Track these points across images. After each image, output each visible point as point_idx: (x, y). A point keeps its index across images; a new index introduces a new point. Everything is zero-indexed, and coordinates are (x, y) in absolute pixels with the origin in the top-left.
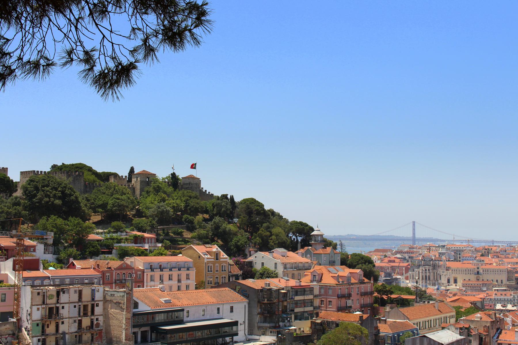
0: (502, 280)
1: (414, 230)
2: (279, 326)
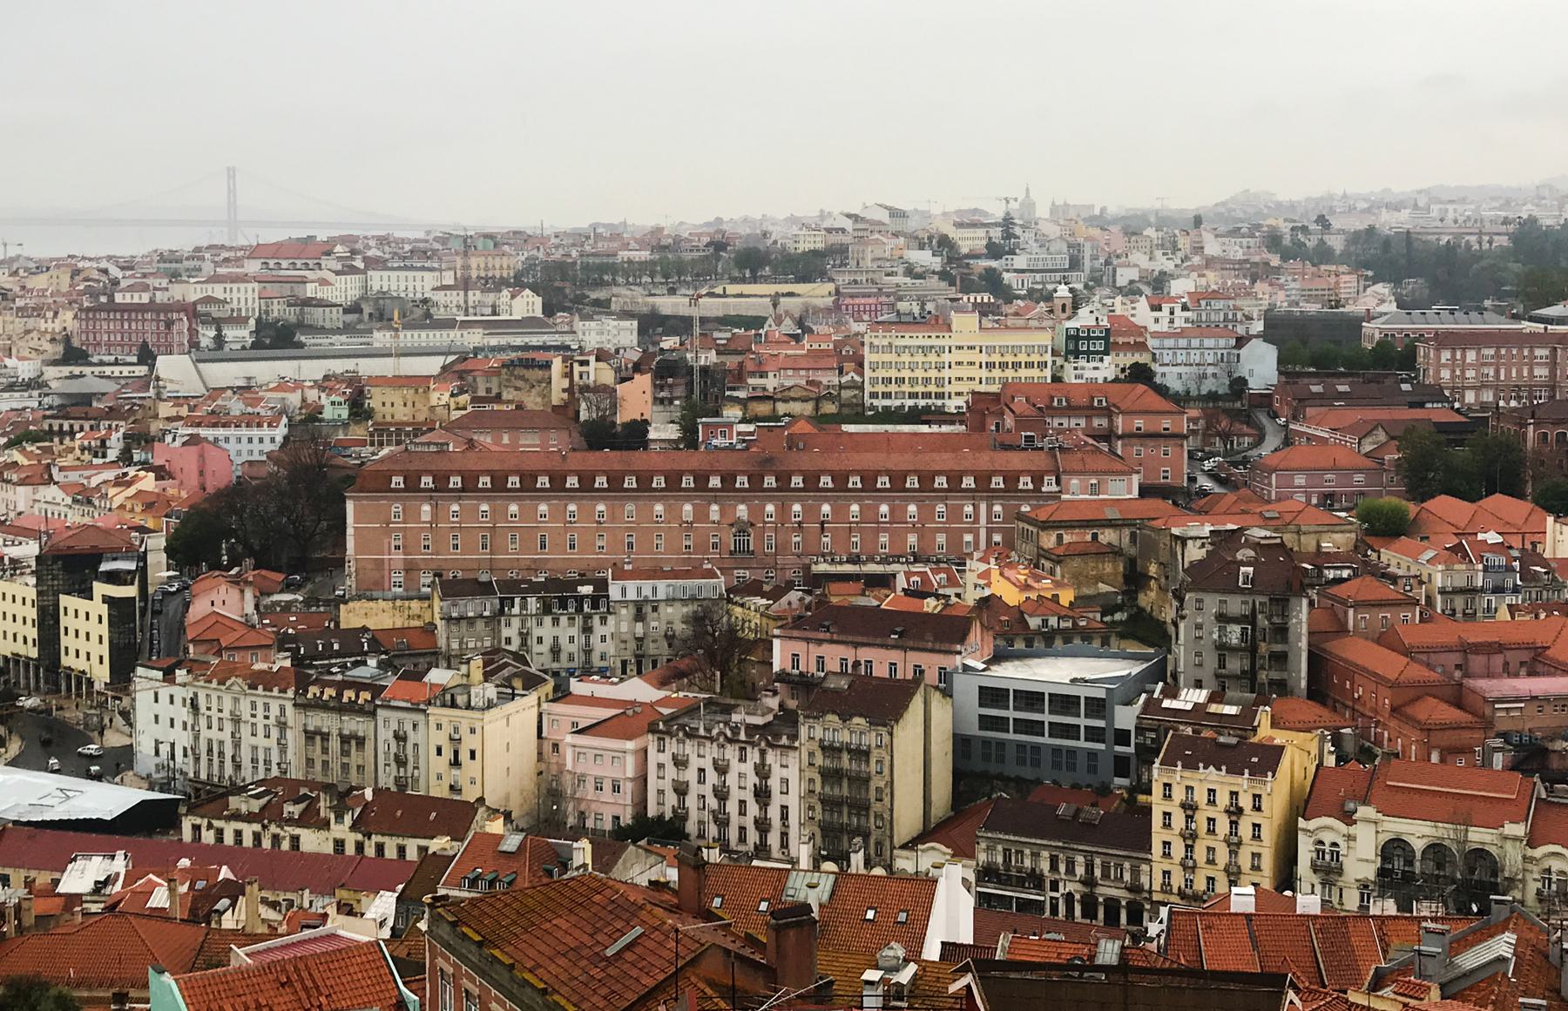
1: (232, 192)
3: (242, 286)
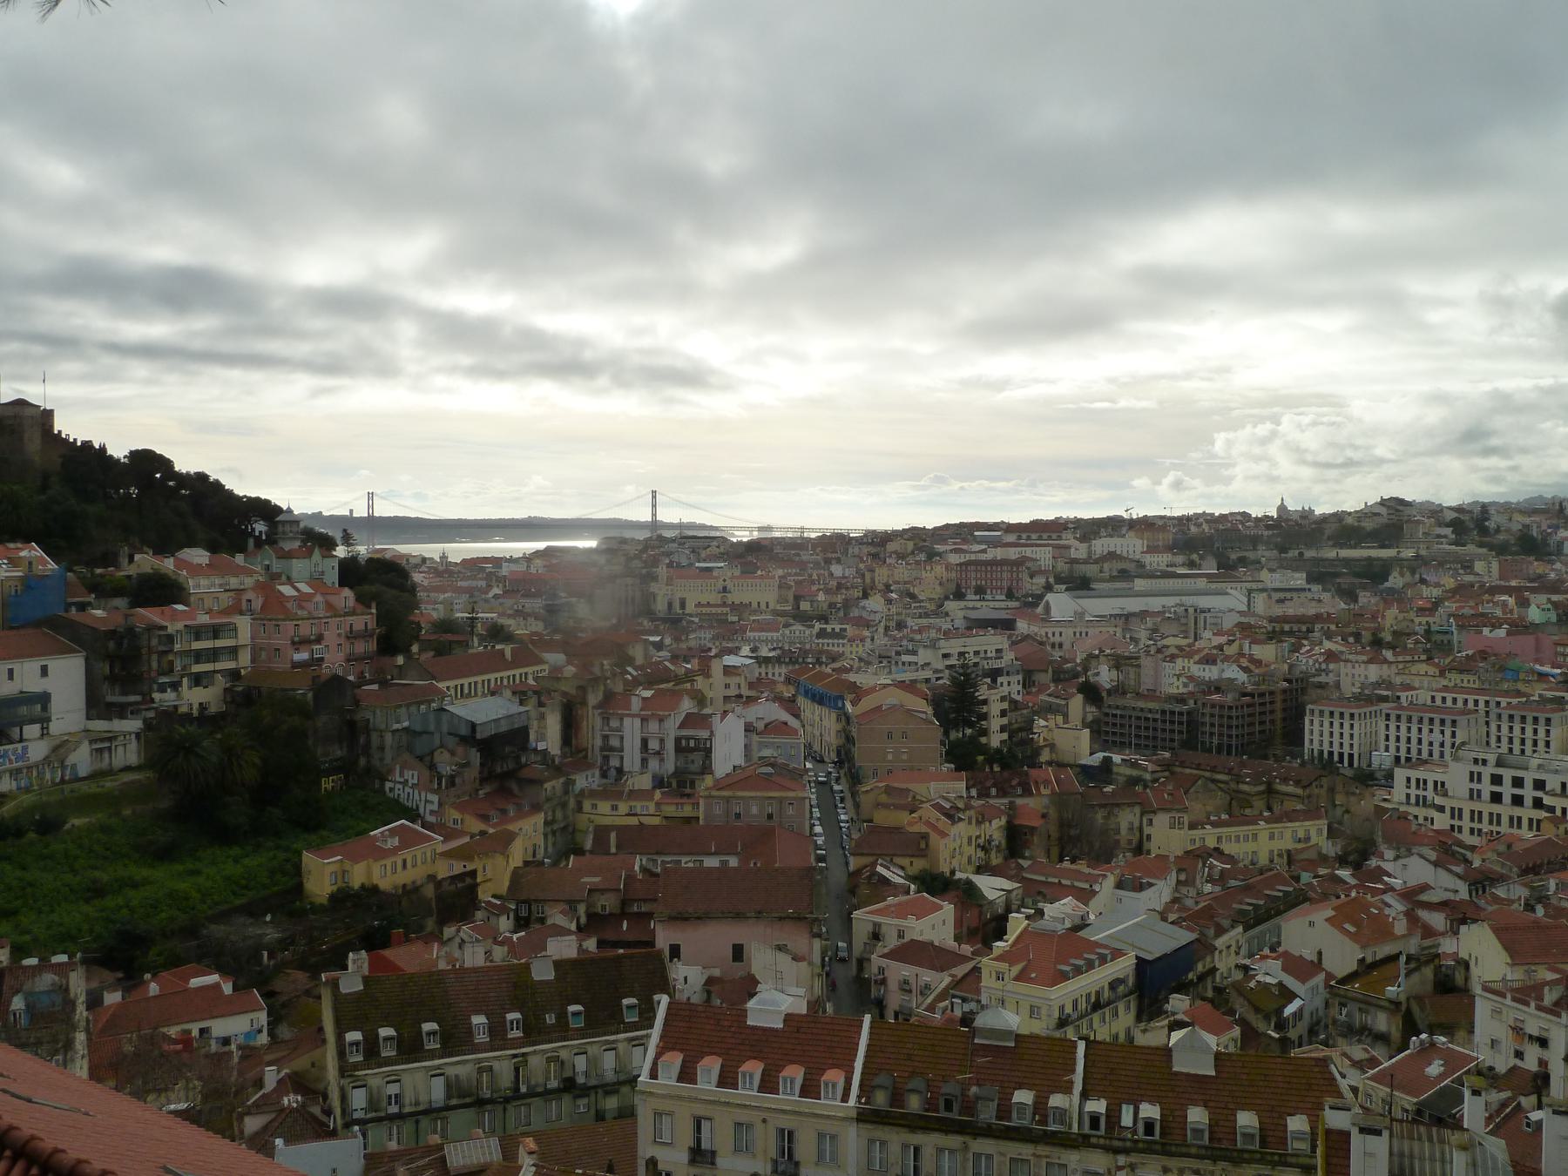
1: (654, 506)
2: (152, 701)
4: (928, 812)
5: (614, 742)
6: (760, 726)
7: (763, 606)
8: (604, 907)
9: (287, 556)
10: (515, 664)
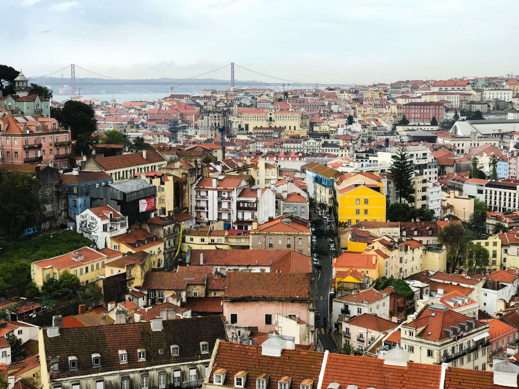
0: (295, 127)
1: (233, 72)
3: (454, 96)
4: (377, 245)
5: (203, 204)
6: (285, 195)
7: (292, 128)
8: (196, 294)
9: (23, 100)
10: (149, 160)
